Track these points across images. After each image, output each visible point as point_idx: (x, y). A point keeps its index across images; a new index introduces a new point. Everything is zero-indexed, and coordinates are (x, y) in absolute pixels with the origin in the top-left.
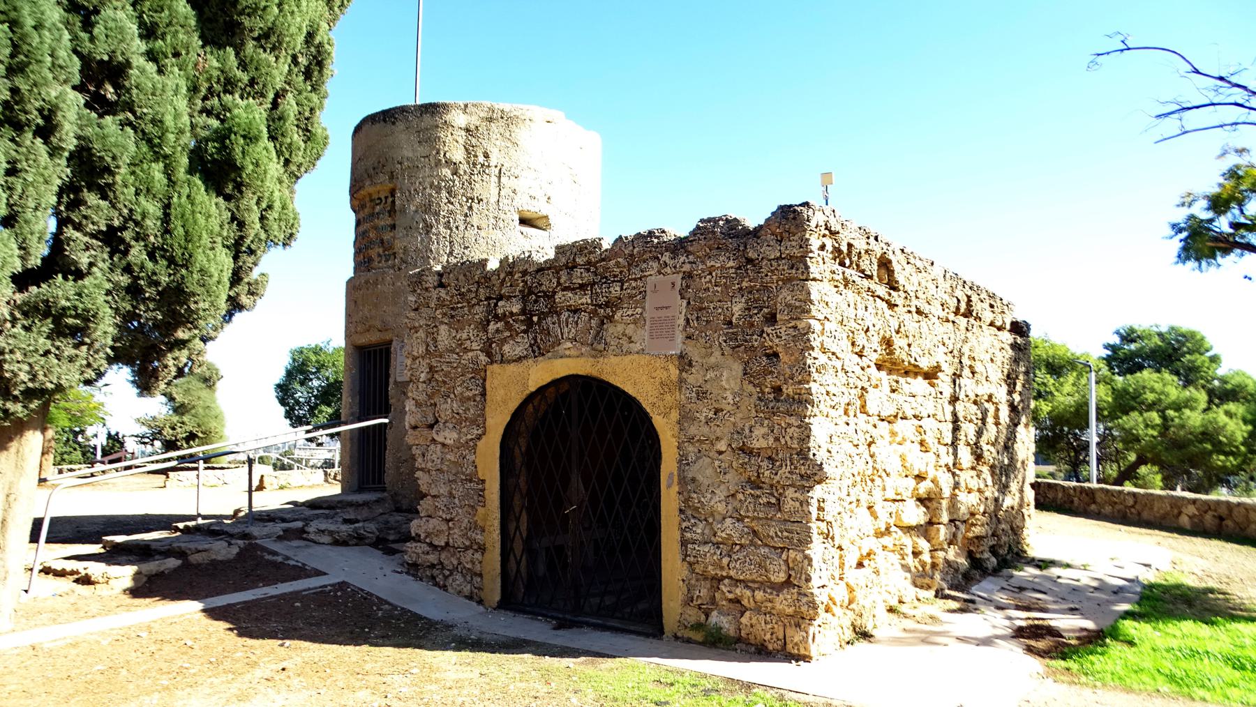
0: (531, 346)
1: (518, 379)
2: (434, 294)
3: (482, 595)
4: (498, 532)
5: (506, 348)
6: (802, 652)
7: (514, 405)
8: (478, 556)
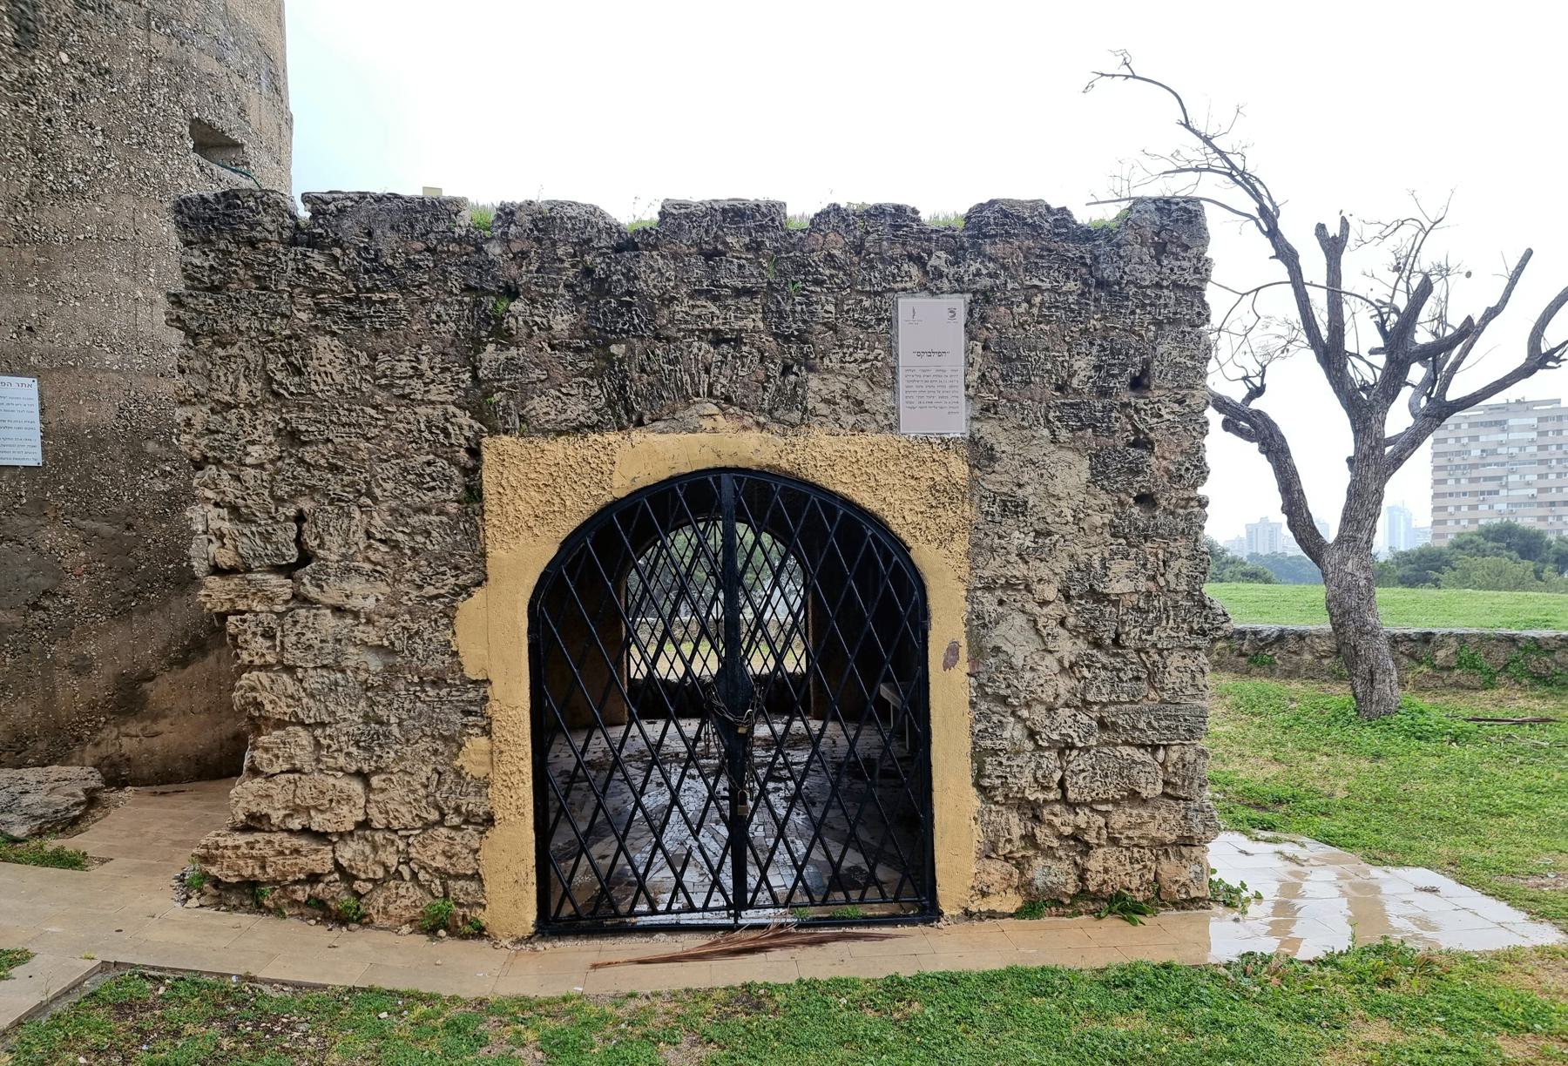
0: (610, 404)
3: (483, 917)
4: (530, 783)
5: (538, 405)
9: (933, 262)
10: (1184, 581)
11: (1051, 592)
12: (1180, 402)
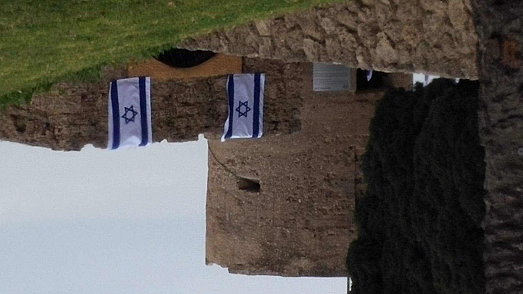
2: (280, 118)
12: (73, 92)
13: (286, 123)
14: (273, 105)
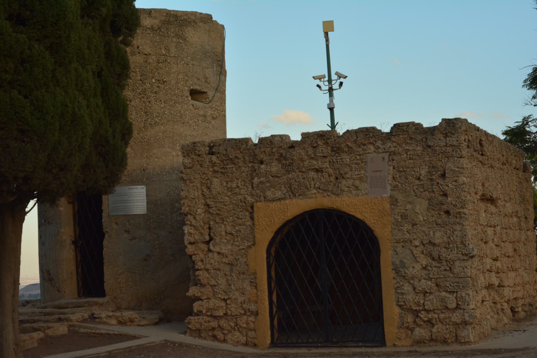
0: (287, 192)
1: (278, 211)
2: (207, 158)
6: (467, 340)
7: (275, 228)
8: (252, 318)
9: (377, 144)
10: (459, 238)
11: (417, 243)
12: (456, 181)
13: (200, 153)
14: (215, 172)
